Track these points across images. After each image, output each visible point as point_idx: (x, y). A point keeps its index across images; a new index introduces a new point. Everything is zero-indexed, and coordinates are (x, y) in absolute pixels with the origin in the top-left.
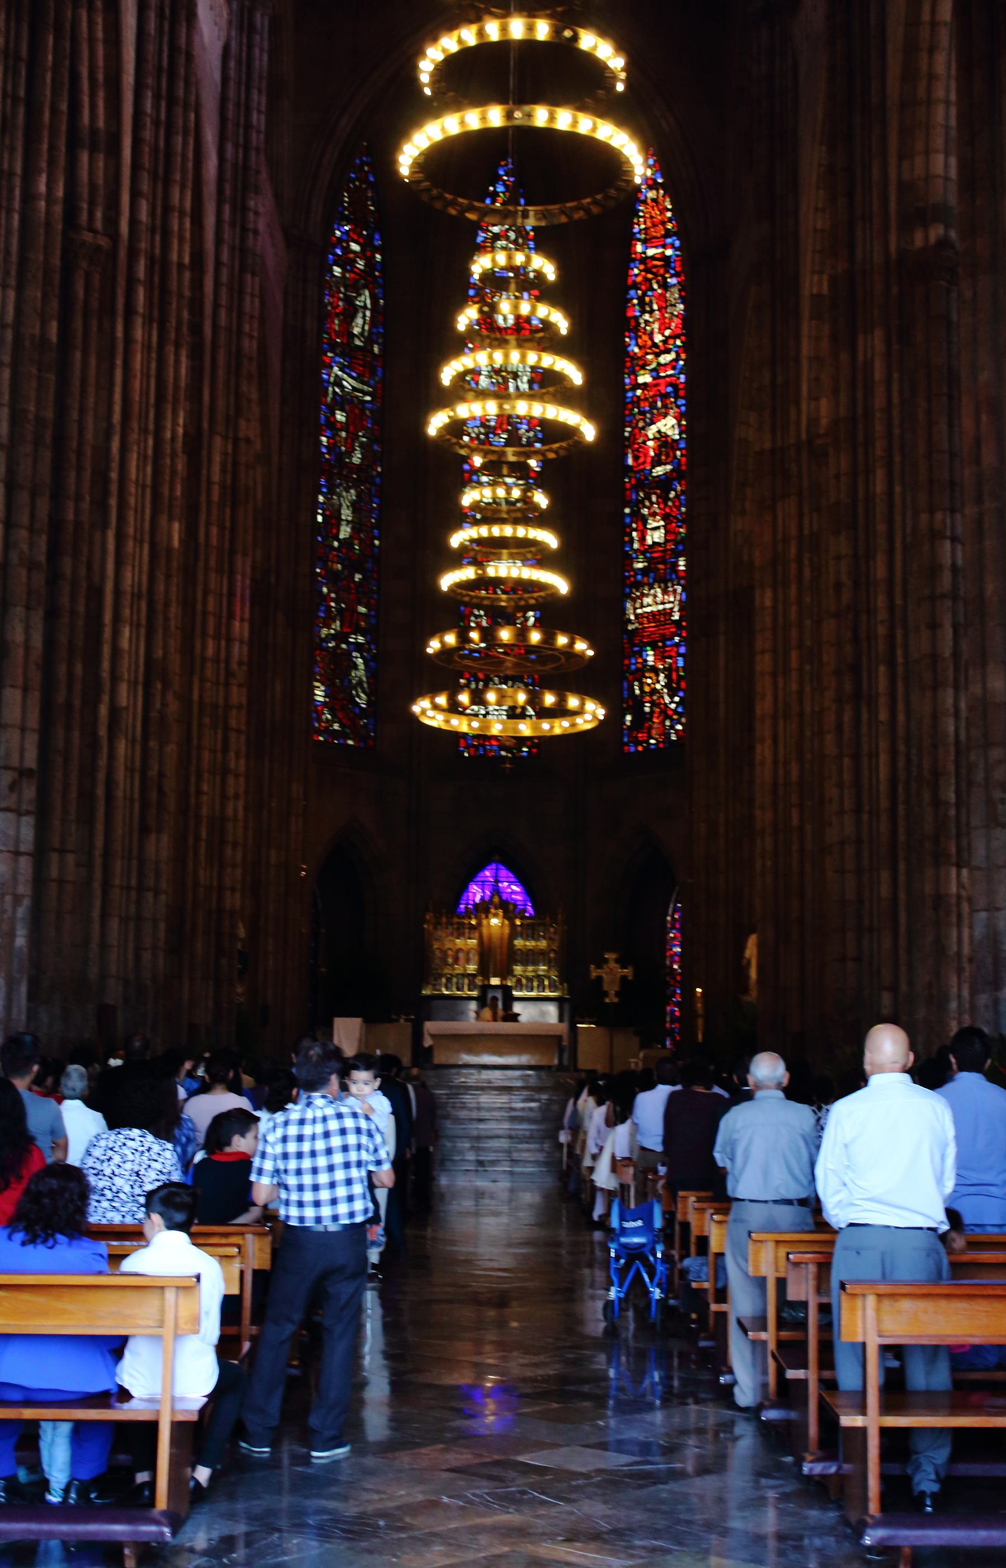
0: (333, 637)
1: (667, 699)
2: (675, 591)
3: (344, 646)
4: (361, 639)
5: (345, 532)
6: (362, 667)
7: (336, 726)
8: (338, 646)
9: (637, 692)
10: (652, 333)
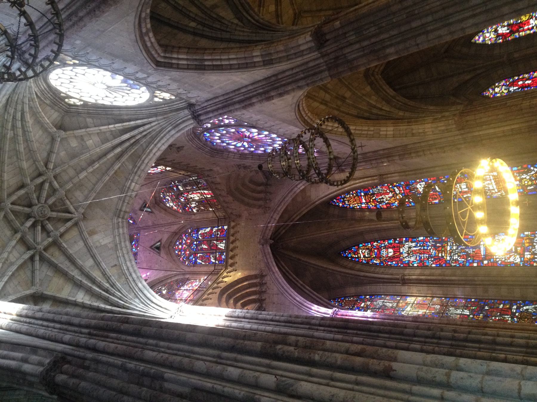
0: (512, 318)
1: (533, 172)
3: (517, 314)
4: (515, 307)
5: (467, 312)
6: (527, 307)
8: (517, 317)
9: (532, 187)
10: (389, 197)
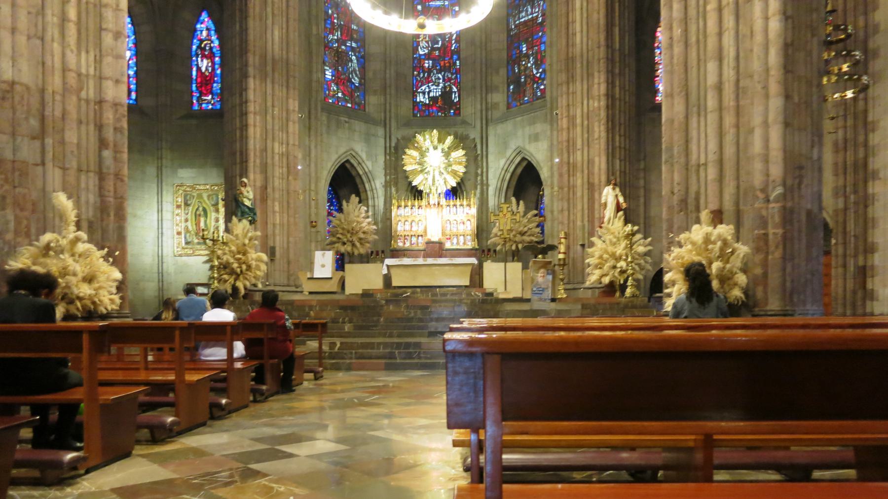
0: (337, 41)
2: (539, 5)
4: (354, 45)
7: (340, 95)
